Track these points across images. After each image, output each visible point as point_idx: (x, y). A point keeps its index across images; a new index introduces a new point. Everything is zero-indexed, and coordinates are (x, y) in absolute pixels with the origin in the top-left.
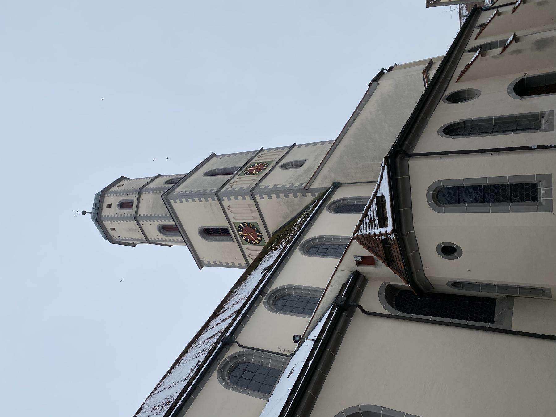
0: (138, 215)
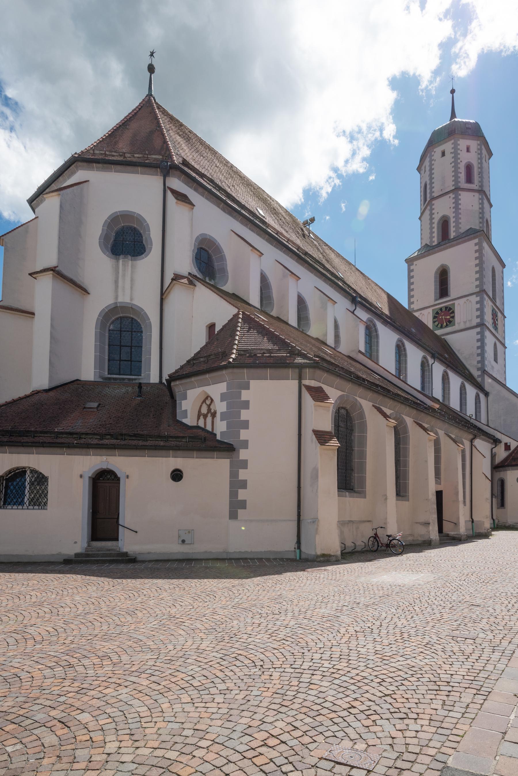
0: (460, 192)
